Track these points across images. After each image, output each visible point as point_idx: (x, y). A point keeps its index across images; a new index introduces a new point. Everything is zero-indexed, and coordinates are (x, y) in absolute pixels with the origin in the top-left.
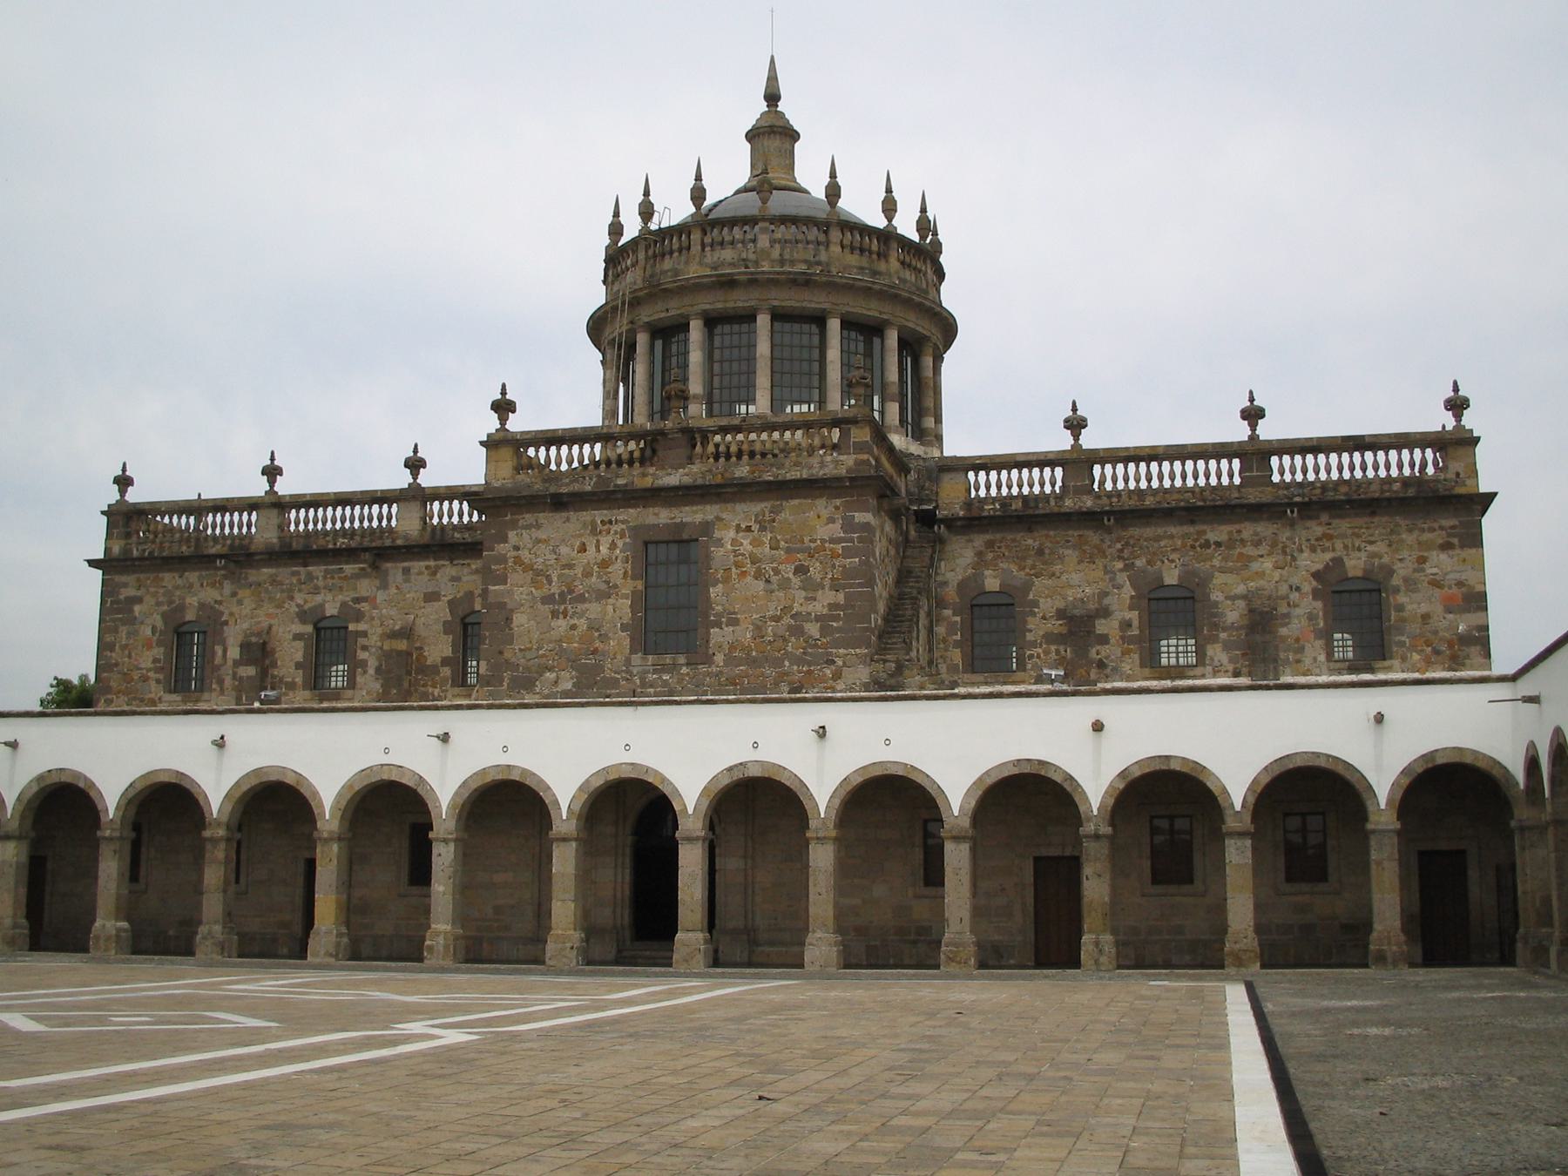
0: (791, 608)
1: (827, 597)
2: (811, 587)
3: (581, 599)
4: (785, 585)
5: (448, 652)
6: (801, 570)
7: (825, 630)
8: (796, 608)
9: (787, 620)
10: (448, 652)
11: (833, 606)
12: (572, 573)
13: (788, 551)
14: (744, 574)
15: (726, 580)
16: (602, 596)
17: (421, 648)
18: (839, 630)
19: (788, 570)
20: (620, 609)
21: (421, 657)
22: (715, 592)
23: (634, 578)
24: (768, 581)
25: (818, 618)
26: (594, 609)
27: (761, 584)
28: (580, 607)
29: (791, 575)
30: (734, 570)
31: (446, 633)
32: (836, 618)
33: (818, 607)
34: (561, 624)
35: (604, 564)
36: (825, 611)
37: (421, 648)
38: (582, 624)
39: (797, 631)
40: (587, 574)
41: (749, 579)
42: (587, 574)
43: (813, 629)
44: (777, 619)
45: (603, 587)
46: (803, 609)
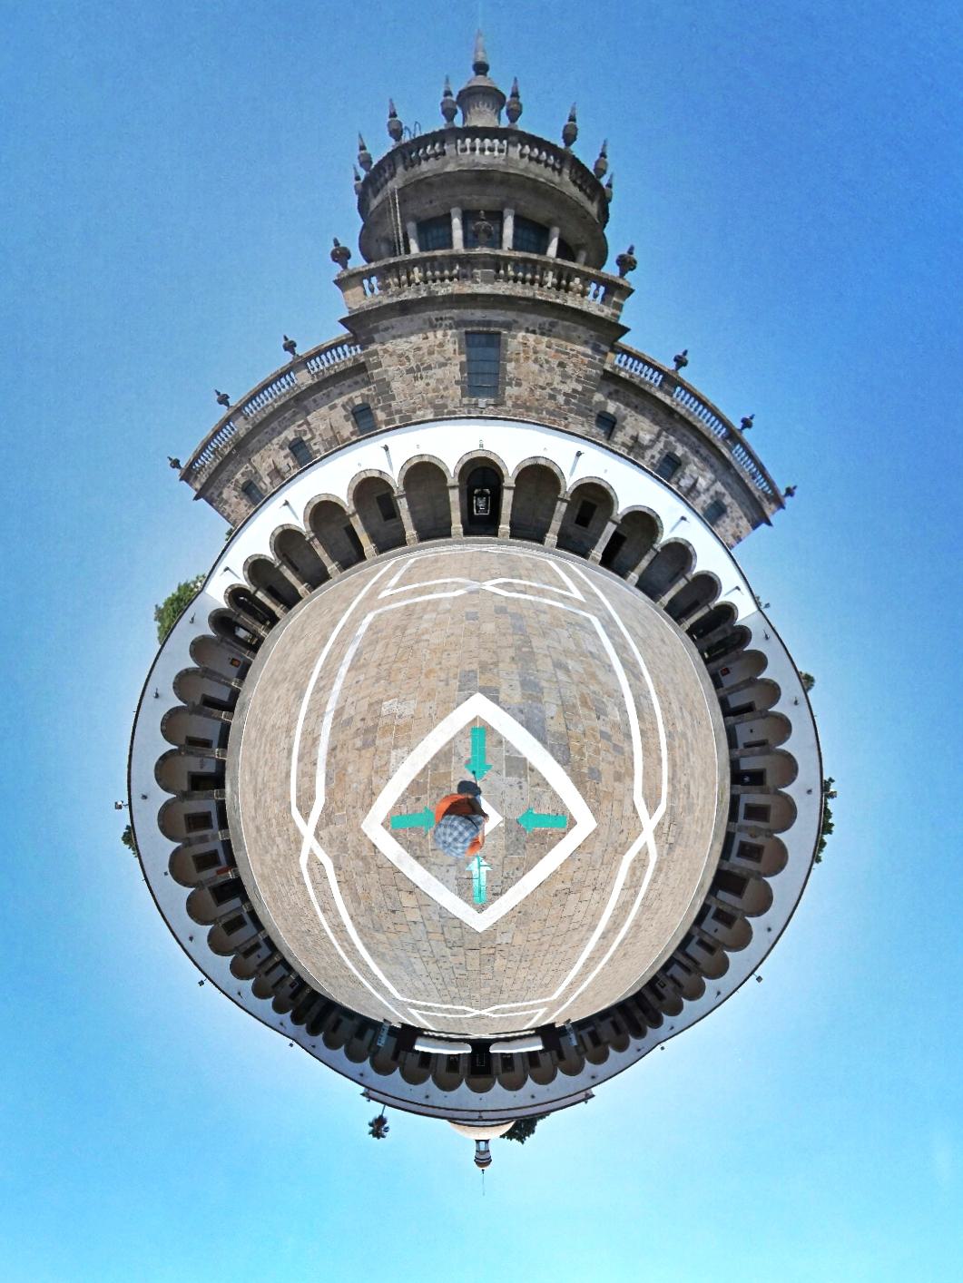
0: (552, 384)
1: (572, 385)
2: (565, 377)
3: (429, 368)
4: (551, 370)
5: (351, 429)
6: (561, 365)
7: (567, 402)
8: (555, 385)
9: (548, 390)
10: (351, 429)
11: (575, 391)
12: (421, 352)
13: (557, 351)
14: (527, 358)
15: (517, 361)
16: (442, 365)
17: (339, 432)
18: (574, 404)
19: (555, 363)
20: (454, 372)
21: (341, 436)
22: (510, 367)
23: (461, 353)
24: (541, 366)
25: (565, 394)
26: (439, 373)
27: (536, 367)
28: (430, 373)
29: (555, 366)
30: (522, 355)
31: (347, 421)
32: (575, 398)
33: (567, 388)
34: (420, 384)
35: (441, 345)
36: (570, 391)
37: (339, 432)
38: (433, 382)
39: (552, 397)
40: (431, 353)
41: (530, 362)
42: (431, 353)
43: (561, 399)
44: (543, 388)
45: (442, 360)
46: (556, 386)
